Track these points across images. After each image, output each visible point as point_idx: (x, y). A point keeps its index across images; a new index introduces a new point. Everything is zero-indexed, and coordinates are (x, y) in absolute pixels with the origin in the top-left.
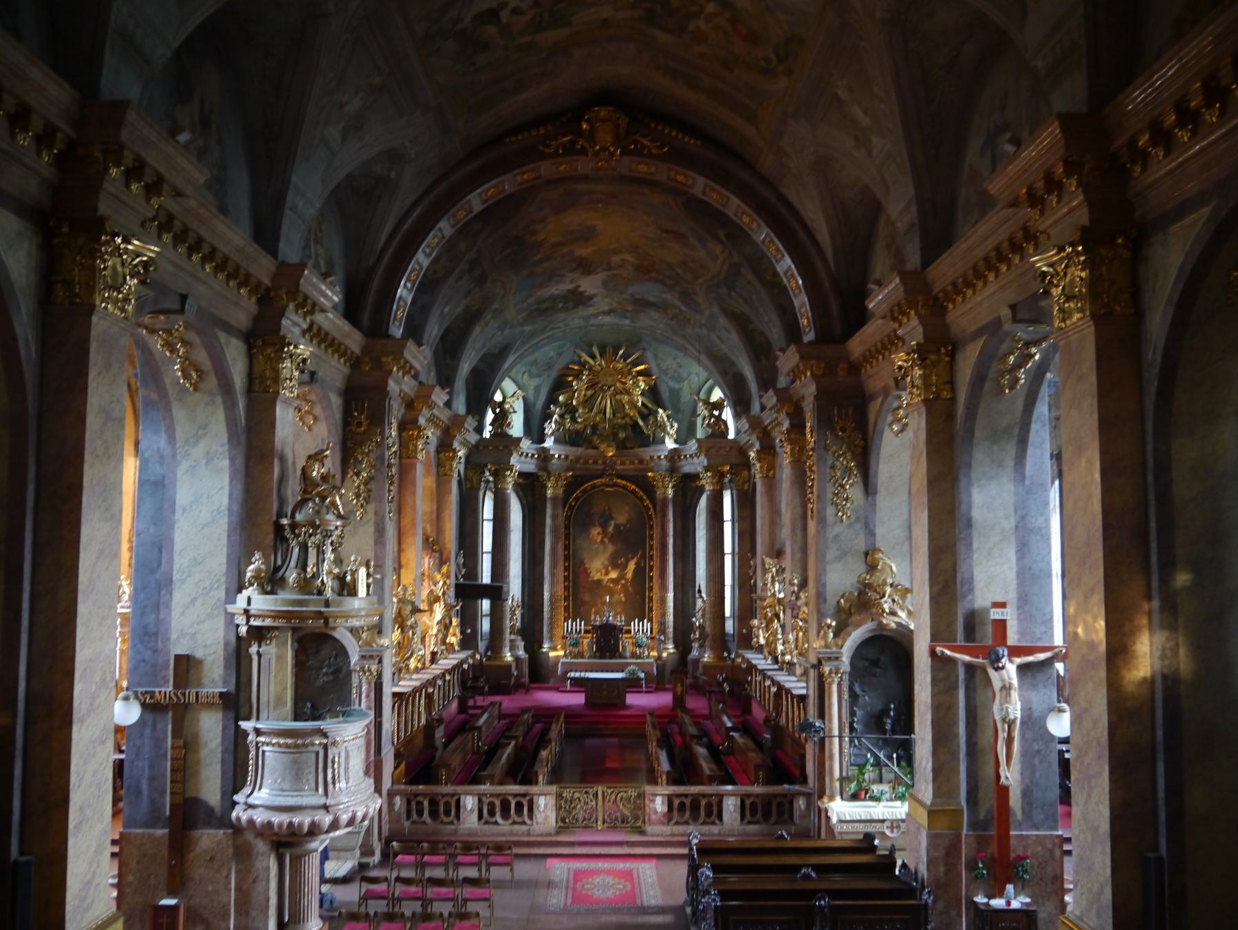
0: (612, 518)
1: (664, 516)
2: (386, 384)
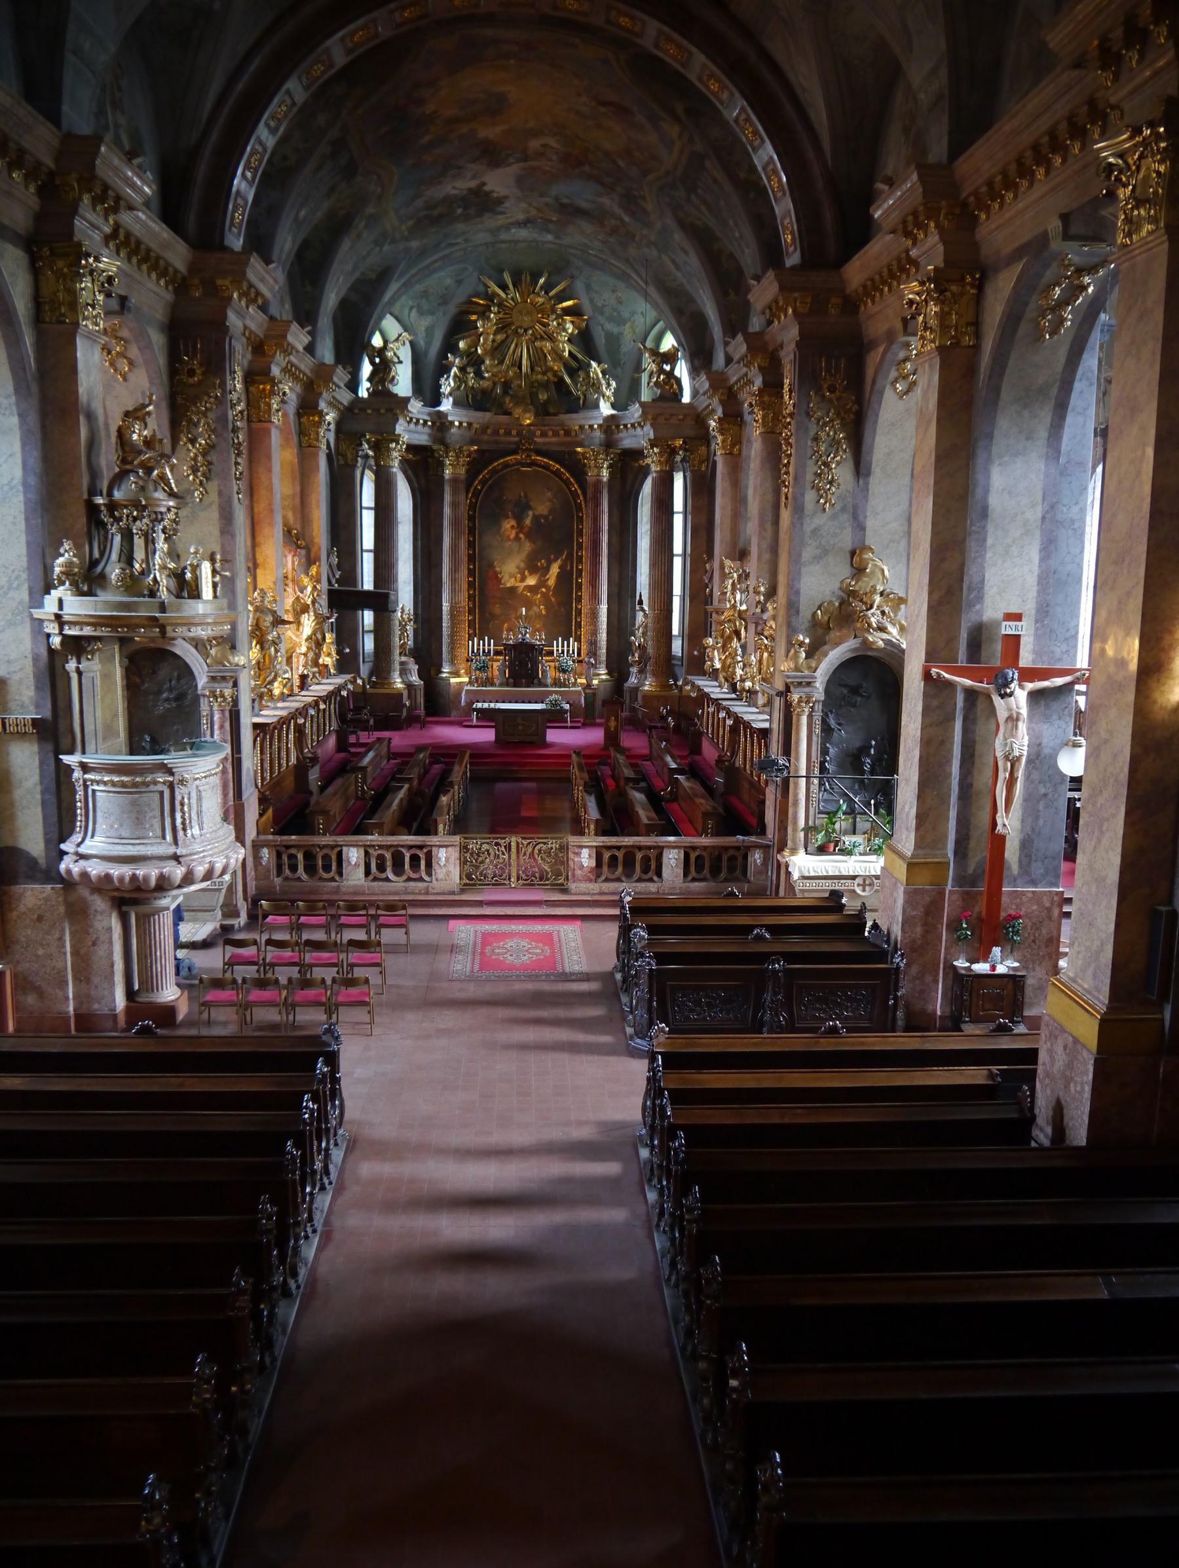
0: (530, 508)
1: (597, 504)
2: (225, 317)
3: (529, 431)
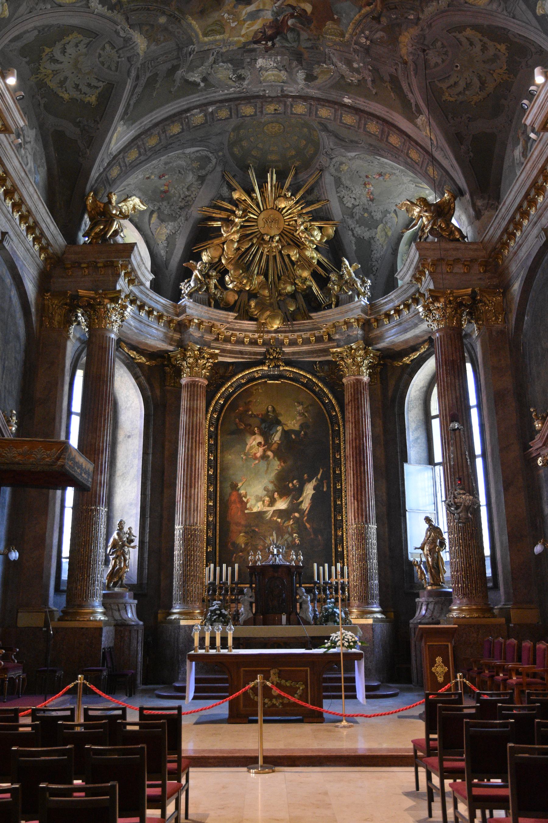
0: (279, 423)
1: (358, 407)
3: (277, 339)
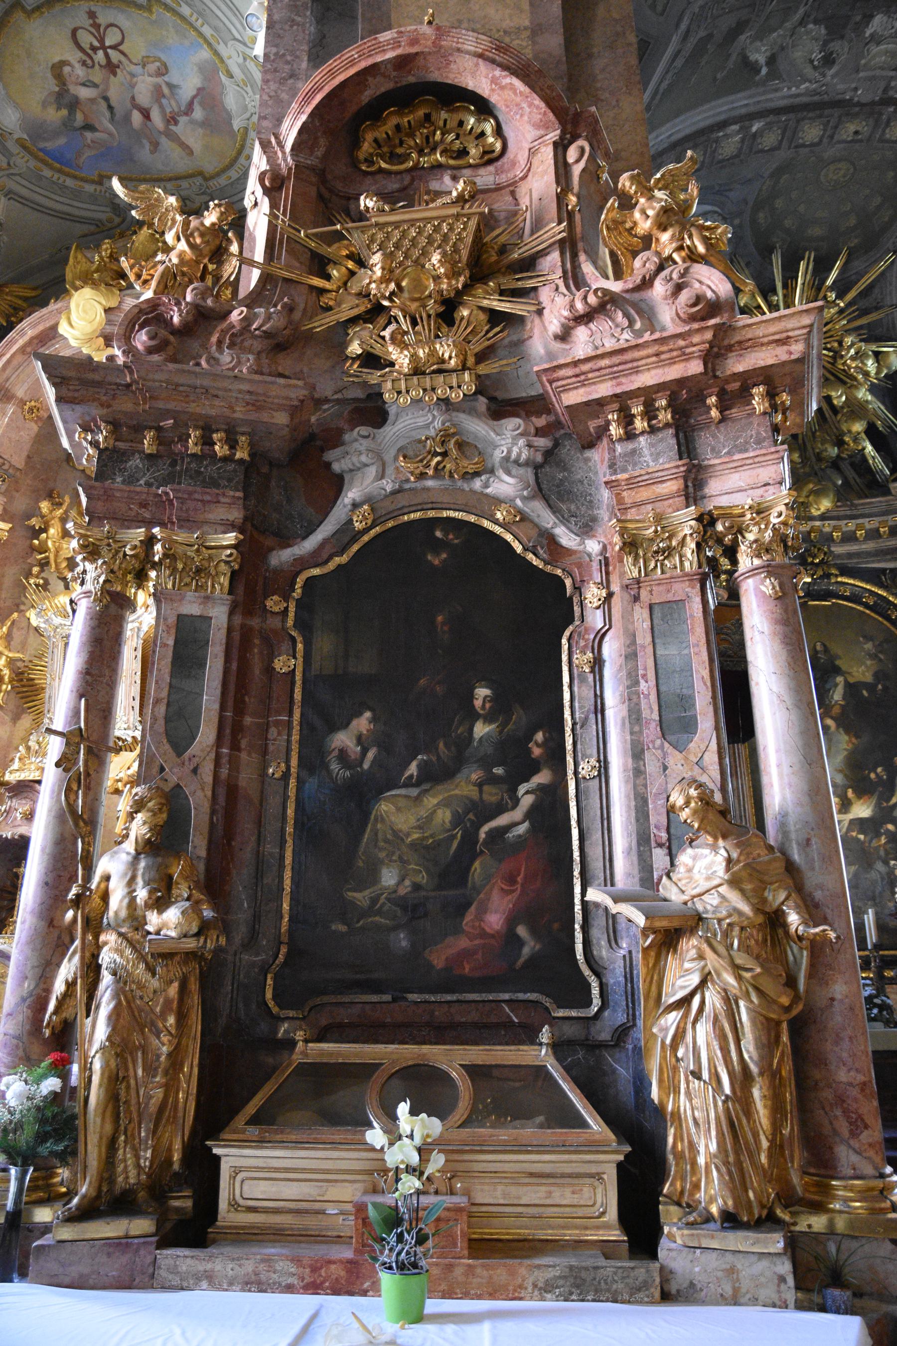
0: (837, 671)
